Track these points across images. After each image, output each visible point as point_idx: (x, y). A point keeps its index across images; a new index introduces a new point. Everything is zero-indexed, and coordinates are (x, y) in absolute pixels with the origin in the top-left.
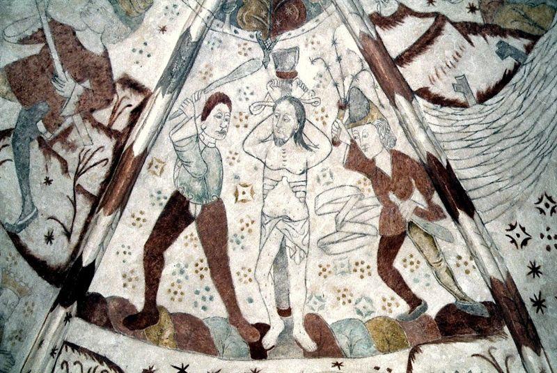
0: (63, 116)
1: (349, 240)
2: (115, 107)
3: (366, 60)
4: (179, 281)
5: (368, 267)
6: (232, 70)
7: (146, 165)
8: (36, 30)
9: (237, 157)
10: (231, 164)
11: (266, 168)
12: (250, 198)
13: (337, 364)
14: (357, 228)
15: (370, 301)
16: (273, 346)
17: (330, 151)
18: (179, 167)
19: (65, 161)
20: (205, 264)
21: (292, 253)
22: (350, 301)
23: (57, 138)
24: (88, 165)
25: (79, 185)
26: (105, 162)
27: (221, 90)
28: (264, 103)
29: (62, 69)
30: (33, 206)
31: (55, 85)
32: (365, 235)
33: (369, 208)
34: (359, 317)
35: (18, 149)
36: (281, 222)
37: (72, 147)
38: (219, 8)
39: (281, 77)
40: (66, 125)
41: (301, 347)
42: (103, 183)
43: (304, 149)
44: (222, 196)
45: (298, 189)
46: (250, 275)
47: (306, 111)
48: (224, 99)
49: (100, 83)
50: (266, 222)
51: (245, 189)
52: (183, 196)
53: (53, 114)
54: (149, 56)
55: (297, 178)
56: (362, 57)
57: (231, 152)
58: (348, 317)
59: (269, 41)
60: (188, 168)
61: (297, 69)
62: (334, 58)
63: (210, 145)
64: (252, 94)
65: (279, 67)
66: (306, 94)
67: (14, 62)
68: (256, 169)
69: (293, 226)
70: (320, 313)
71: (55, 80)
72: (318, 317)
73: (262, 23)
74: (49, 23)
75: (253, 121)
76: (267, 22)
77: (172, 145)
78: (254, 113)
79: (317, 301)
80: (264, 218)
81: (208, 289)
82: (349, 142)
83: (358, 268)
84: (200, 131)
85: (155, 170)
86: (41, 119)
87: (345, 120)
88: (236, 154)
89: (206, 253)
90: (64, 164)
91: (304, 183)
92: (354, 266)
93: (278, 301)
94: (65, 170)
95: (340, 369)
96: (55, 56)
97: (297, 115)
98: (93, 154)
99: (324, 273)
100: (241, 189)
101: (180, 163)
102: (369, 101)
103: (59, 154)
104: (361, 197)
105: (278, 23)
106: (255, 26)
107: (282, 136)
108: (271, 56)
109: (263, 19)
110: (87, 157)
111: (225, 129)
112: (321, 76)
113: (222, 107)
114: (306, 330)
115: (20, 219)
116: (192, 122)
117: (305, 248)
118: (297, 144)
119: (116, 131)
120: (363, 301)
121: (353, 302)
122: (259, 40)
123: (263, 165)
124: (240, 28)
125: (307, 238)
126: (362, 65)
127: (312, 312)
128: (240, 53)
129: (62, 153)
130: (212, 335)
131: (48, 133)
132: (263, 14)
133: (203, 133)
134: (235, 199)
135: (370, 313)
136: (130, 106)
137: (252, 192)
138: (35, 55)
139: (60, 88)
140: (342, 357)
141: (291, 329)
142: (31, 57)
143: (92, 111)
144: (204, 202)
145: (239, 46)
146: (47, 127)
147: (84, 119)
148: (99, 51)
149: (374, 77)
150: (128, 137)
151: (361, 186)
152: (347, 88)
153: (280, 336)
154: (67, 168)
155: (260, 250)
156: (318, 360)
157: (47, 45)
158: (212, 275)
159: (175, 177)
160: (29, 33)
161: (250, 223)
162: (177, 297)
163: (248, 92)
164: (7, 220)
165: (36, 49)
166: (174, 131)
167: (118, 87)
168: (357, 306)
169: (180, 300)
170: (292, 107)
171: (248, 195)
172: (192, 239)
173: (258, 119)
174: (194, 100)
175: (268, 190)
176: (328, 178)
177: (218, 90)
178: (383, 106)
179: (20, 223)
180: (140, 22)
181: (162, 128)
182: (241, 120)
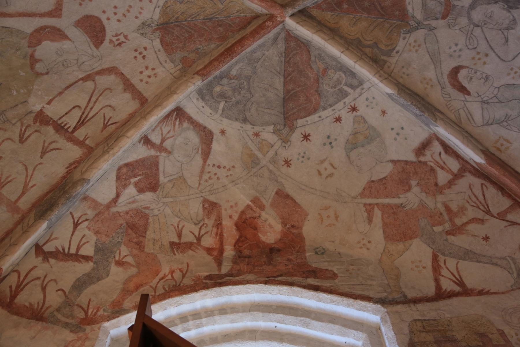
0: (435, 209)
2: (438, 166)
6: (430, 61)
7: (497, 153)
8: (364, 209)
18: (509, 125)
19: (473, 219)
23: (451, 220)
24: (483, 201)
25: (498, 214)
26: (484, 186)
27: (446, 72)
28: (469, 34)
29: (398, 199)
30: (504, 258)
31: (407, 208)
35: (451, 253)
37: (462, 210)
38: (375, 66)
39: (447, 16)
40: (443, 210)
42: (503, 194)
48: (456, 71)
49: (416, 173)
53: (431, 217)
54: (402, 128)
57: (509, 74)
59: (412, 23)
63: (495, 93)
64: (456, 45)
65: (438, 16)
67: (384, 232)
71: (405, 207)
73: (394, 28)
74: (361, 198)
75: (483, 47)
76: (395, 23)
77: (486, 127)
78: (475, 46)
84: (479, 99)
85: (504, 147)
86: (432, 227)
88: (512, 69)
90: (474, 220)
94: (482, 221)
96: (387, 201)
98: (474, 194)
103: (465, 222)
105: (397, 13)
106: (396, 34)
107: (507, 21)
108: (425, 23)
109: (391, 26)
110: (474, 199)
111: (484, 75)
115: (511, 274)
116: (468, 104)
119: (459, 170)
122: (409, 32)
124: (395, 48)
128: (417, 51)
129: (465, 220)
131: (445, 225)
132: (386, 25)
133: (482, 97)
136: (440, 154)
138: (382, 215)
139: (410, 206)
142: (383, 220)
143: (436, 184)
145: (410, 51)
146: (440, 224)
147: (441, 193)
148: (390, 167)
150: (467, 162)
154: (480, 219)
157: (377, 204)
159: (517, 131)
160: (365, 214)
163: (454, 48)
164: (509, 285)
165: (377, 213)
166: (472, 122)
167: (422, 159)
170: (478, 8)
174: (449, 99)
177: (445, 77)
179: (515, 275)
180: (374, 129)
181: (467, 132)
182: (479, 59)
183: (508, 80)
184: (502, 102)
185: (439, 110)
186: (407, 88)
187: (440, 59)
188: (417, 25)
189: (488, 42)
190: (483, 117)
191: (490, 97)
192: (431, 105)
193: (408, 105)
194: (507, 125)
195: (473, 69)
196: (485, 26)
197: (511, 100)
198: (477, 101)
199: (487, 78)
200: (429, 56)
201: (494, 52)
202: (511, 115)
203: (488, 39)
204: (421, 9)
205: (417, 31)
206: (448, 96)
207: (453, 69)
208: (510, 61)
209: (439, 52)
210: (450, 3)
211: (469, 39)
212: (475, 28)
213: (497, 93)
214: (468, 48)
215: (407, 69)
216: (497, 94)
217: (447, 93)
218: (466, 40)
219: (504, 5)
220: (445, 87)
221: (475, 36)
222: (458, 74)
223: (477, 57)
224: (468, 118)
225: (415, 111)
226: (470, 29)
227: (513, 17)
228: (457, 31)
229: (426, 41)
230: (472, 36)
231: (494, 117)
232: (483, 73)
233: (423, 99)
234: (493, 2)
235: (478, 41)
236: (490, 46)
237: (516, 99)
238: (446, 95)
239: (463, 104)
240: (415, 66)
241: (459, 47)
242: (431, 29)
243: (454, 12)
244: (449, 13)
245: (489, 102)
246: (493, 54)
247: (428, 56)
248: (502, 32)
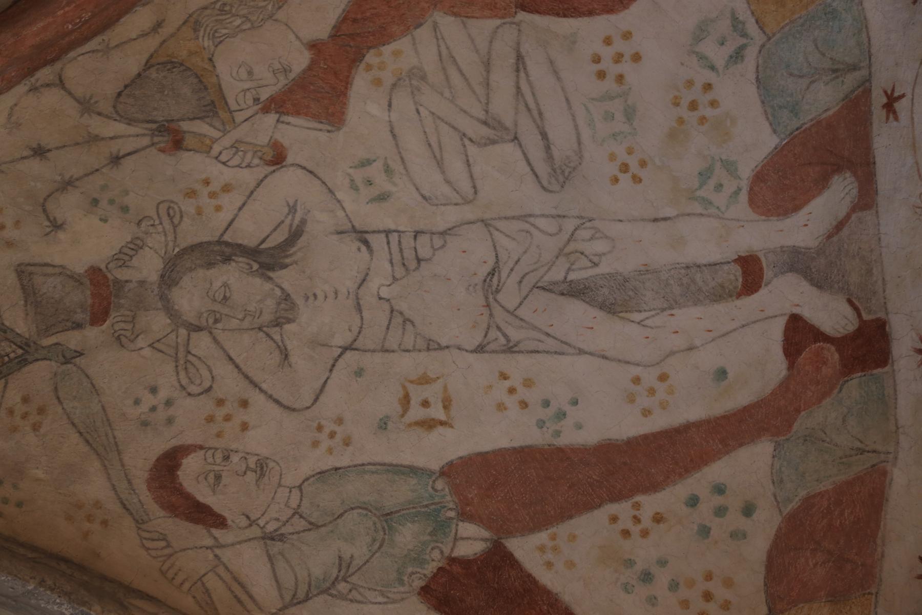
1: (537, 104)
3: (31, 72)
4: (674, 586)
5: (608, 41)
9: (329, 427)
10: (347, 442)
11: (356, 345)
12: (437, 387)
13: (890, 106)
14: (503, 80)
15: (701, 32)
16: (850, 302)
17: (299, 172)
20: (623, 509)
21: (584, 262)
22: (708, 87)
28: (181, 355)
32: (520, 58)
33: (444, 52)
34: (751, 54)
36: (500, 297)
41: (848, 217)
43: (302, 242)
44: (435, 466)
45: (409, 254)
46: (649, 377)
47: (197, 240)
50: (502, 340)
51: (415, 401)
52: (435, 576)
55: (382, 265)
56: (21, 88)
57: (315, 444)
58: (752, 91)
60: (357, 562)
61: (80, 269)
62: (35, 166)
63: (294, 503)
64: (154, 390)
65: (79, 317)
66: (149, 242)
68: (359, 373)
69: (511, 264)
70: (746, 171)
72: (759, 177)
78: (207, 384)
79: (712, 183)
80: (492, 346)
81: (693, 501)
82: (272, 118)
83: (613, 70)
84: (255, 531)
87: (215, 134)
89: (589, 506)
91: (394, 238)
92: (609, 84)
93: (720, 295)
95: (903, 96)
97: (210, 265)
99: (634, 167)
100: (416, 413)
101: (342, 587)
102: (148, 65)
104: (418, 75)
107: (270, 303)
111: (252, 461)
112: (95, 202)
113: (190, 466)
114: (797, 209)
116: (226, 555)
117: (569, 225)
118: (288, 261)
120: (703, 48)
121: (710, 76)
123: (348, 355)
125: (542, 223)
126: (48, 85)
127: (744, 197)
128: (36, 427)
130: (826, 486)
134: (440, 429)
135: (737, 25)
137: (424, 380)
140: (868, 92)
141: (795, 251)
144: (452, 514)
145: (15, 429)
149: (81, 50)
151: (388, 78)
152: (120, 128)
153: (819, 283)
155: (581, 352)
156: (878, 165)
158: (653, 487)
159: (380, 599)
161: (507, 384)
162: (721, 593)
163: (148, 400)
168: (720, 63)
169: (728, 583)
170: (186, 281)
171: (432, 392)
172: (555, 549)
173: (223, 370)
174: (167, 551)
175: (417, 335)
176: (375, 171)
178: (159, 25)
182: (228, 418)
183: (318, 460)
184: (318, 527)
185: (140, 591)
186: (22, 545)
187: (115, 438)
188: (20, 352)
189: (237, 367)
190: (277, 581)
191: (284, 519)
192: (112, 581)
193: (29, 592)
194: (350, 591)
195: (216, 449)
196: (219, 326)
197: (341, 515)
198: (250, 540)
199: (261, 468)
200: (77, 435)
201: (261, 390)
202: (352, 557)
203: (238, 361)
204: (22, 302)
205: (26, 369)
206: (163, 544)
207: (158, 460)
208: (308, 408)
209: (108, 420)
210: (105, 277)
211: (186, 368)
212: (194, 335)
213: (298, 502)
214: (189, 394)
215: (15, 486)
216: (299, 506)
217: (156, 536)
218: (178, 373)
219: (248, 264)
220: (145, 518)
221: (200, 358)
222: (179, 473)
223: (220, 413)
224: (236, 597)
225: (55, 608)
226: (179, 340)
227: (282, 289)
228: (147, 352)
229: (61, 394)
230: (190, 358)
231: (309, 575)
232: (248, 453)
233: (81, 568)
234: (218, 258)
235: (211, 371)
236: (247, 377)
237: (352, 509)
238: (153, 540)
239: (211, 556)
240: (40, 474)
241: (163, 394)
242: (68, 355)
243: (122, 301)
244: (109, 304)
245: (282, 535)
246: (262, 397)
247: (74, 437)
248: (268, 335)
